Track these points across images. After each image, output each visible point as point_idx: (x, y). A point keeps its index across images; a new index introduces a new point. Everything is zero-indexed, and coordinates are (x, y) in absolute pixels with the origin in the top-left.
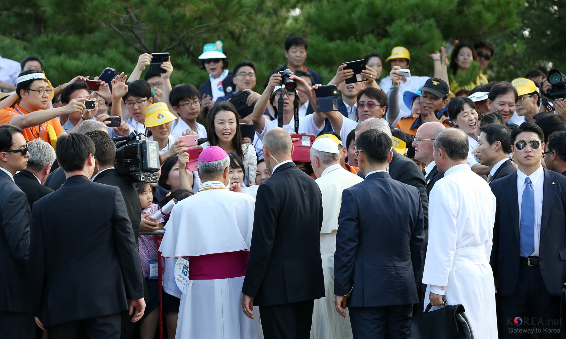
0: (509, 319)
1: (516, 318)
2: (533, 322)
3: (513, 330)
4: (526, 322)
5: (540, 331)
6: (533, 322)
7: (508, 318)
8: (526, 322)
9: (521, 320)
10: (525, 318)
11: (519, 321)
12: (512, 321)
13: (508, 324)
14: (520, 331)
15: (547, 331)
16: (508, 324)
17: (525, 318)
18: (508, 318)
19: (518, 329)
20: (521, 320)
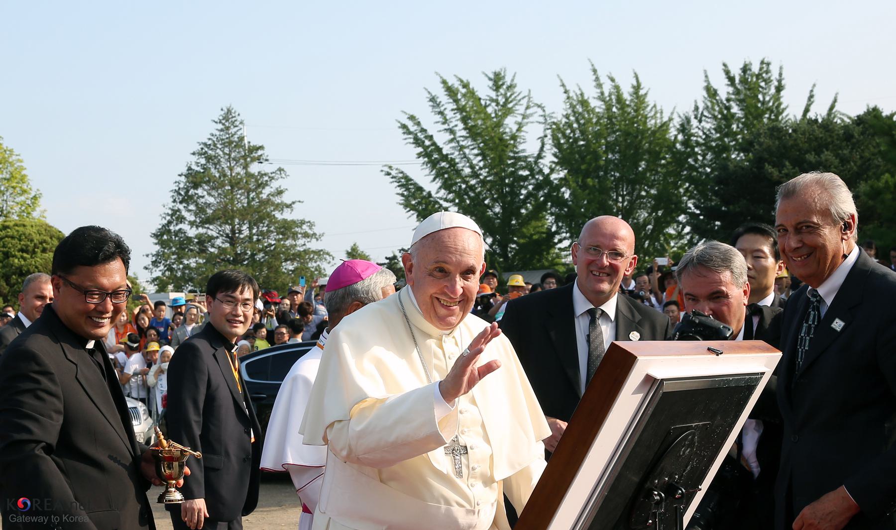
0: (10, 502)
1: (21, 499)
2: (47, 506)
3: (16, 517)
4: (37, 505)
5: (57, 519)
6: (47, 506)
7: (8, 500)
8: (37, 505)
9: (29, 503)
10: (34, 500)
11: (25, 504)
12: (15, 504)
13: (8, 509)
14: (27, 519)
15: (69, 520)
16: (8, 509)
17: (34, 500)
18: (8, 500)
19: (23, 517)
20: (29, 503)
